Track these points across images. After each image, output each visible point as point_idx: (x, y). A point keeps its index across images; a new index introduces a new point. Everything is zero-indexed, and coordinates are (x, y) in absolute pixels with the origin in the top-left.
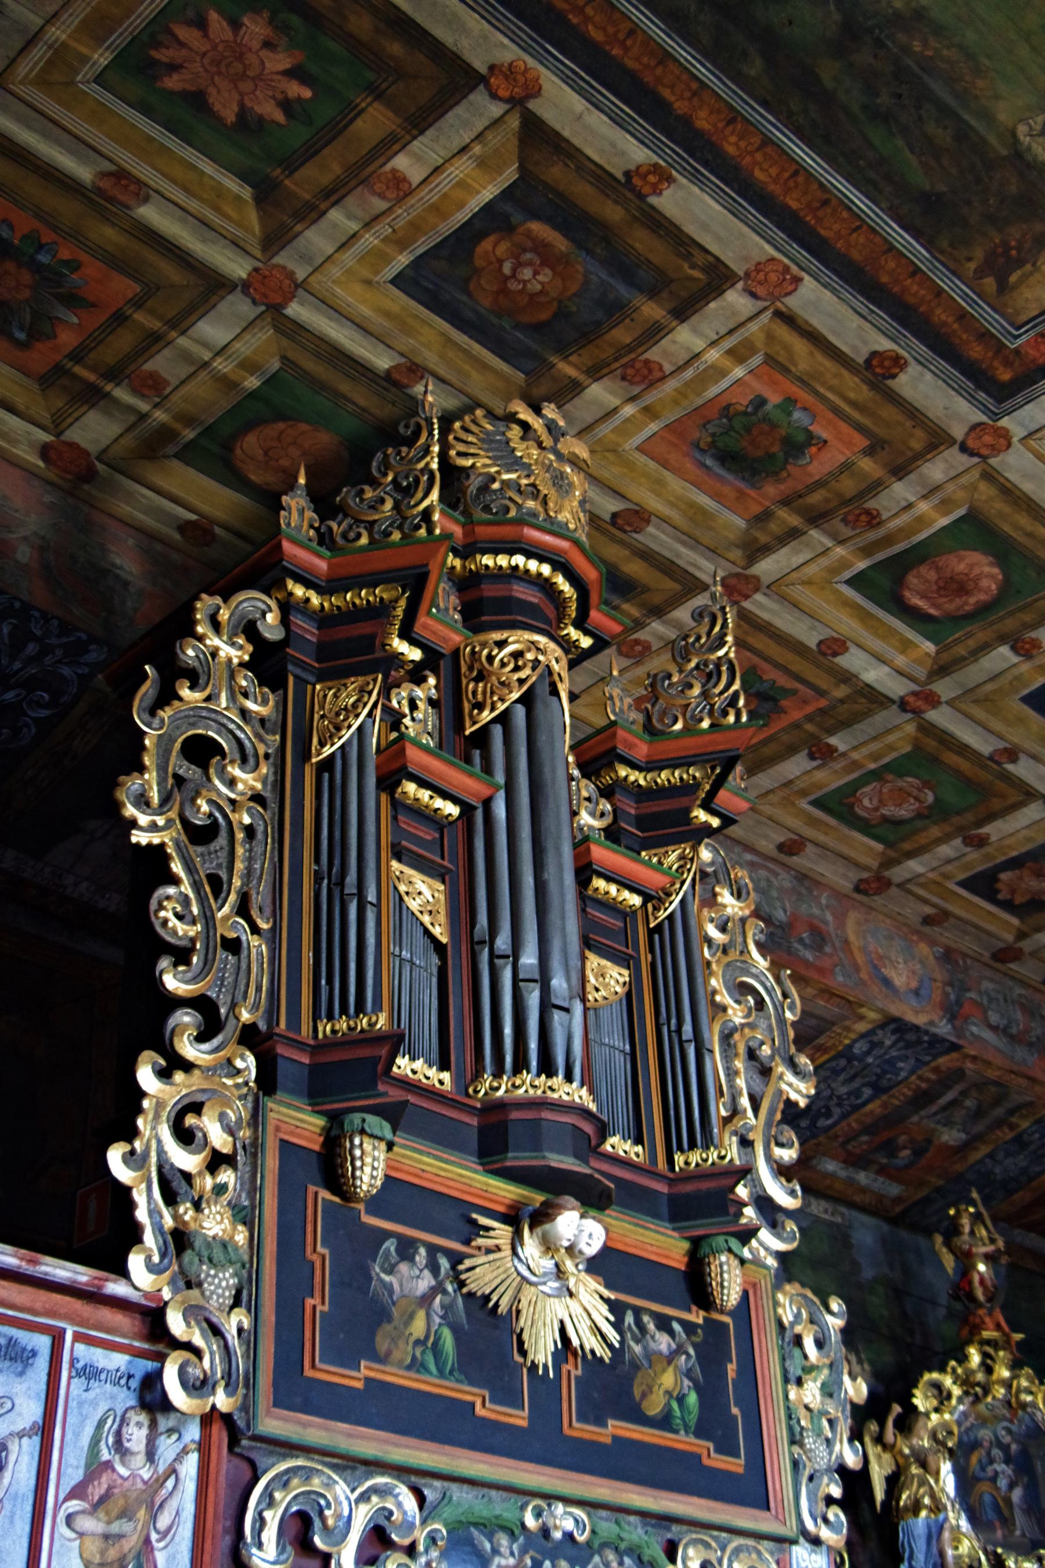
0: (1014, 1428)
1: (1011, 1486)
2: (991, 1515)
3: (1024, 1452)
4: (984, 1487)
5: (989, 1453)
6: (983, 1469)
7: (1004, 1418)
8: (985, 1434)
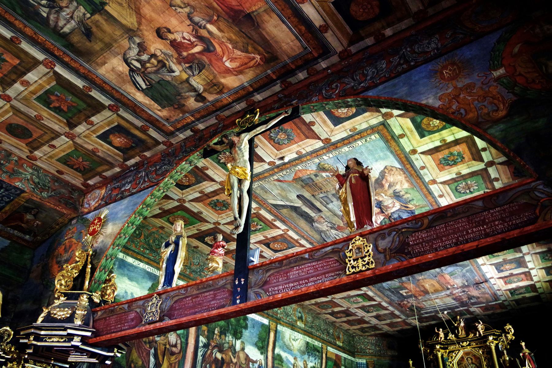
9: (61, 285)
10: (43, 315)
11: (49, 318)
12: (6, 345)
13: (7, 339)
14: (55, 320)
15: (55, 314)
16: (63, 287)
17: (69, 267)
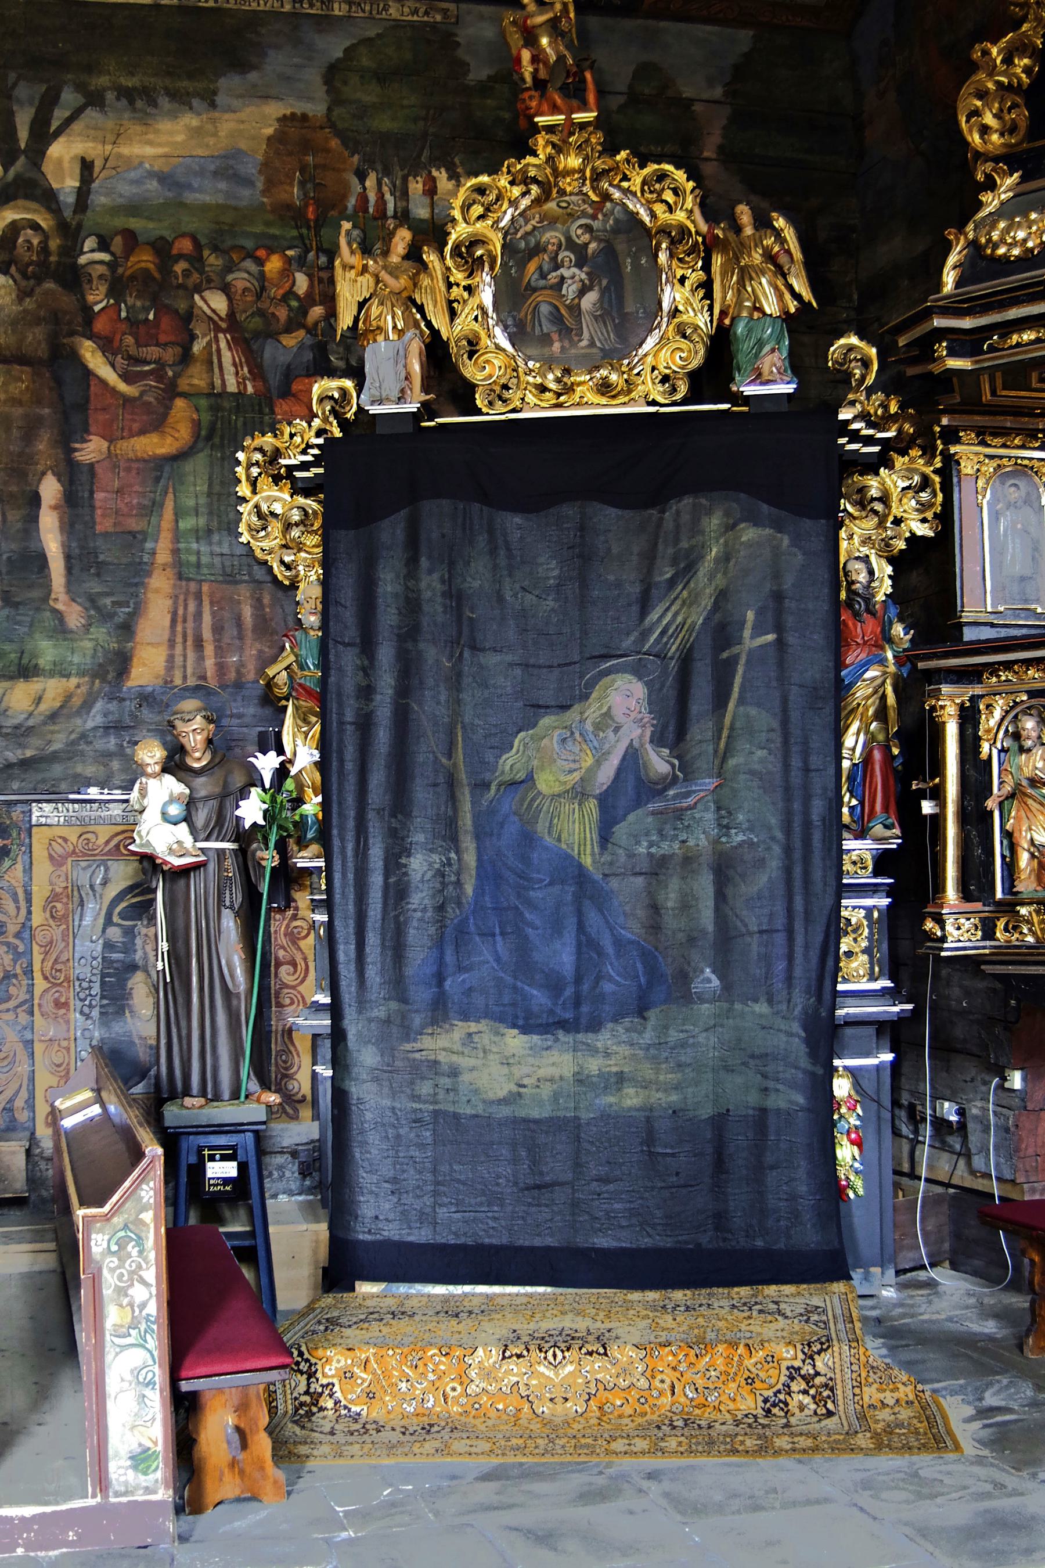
0: (596, 225)
1: (582, 292)
2: (547, 327)
3: (609, 252)
4: (539, 297)
5: (554, 258)
6: (543, 276)
7: (584, 214)
8: (552, 237)
9: (985, 130)
10: (952, 259)
11: (981, 264)
12: (868, 398)
13: (863, 378)
14: (1006, 266)
15: (996, 246)
16: (995, 137)
17: (994, 51)
